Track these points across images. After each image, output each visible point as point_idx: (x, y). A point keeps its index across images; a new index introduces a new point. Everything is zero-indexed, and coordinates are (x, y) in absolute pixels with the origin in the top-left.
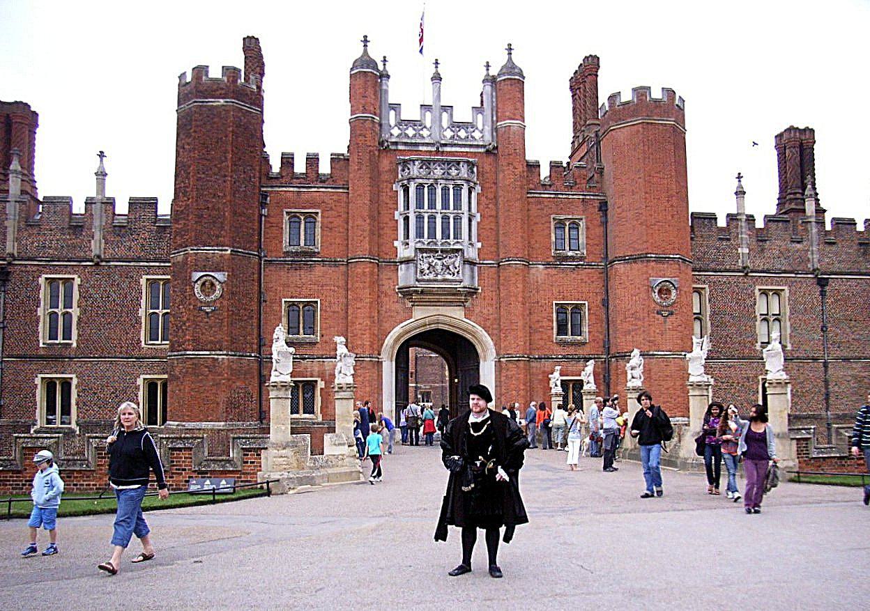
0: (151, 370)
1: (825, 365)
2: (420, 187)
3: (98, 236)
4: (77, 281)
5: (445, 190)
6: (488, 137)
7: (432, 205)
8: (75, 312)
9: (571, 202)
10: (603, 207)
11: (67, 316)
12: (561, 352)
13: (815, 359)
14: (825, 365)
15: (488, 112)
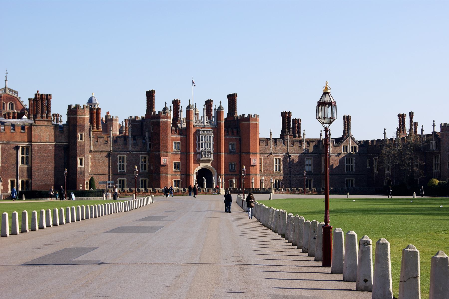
0: (142, 177)
1: (290, 176)
2: (202, 136)
3: (130, 146)
4: (126, 156)
5: (207, 137)
6: (216, 124)
7: (205, 140)
8: (125, 164)
9: (233, 139)
10: (240, 140)
11: (123, 165)
12: (230, 173)
13: (287, 175)
14: (290, 176)
15: (216, 118)
